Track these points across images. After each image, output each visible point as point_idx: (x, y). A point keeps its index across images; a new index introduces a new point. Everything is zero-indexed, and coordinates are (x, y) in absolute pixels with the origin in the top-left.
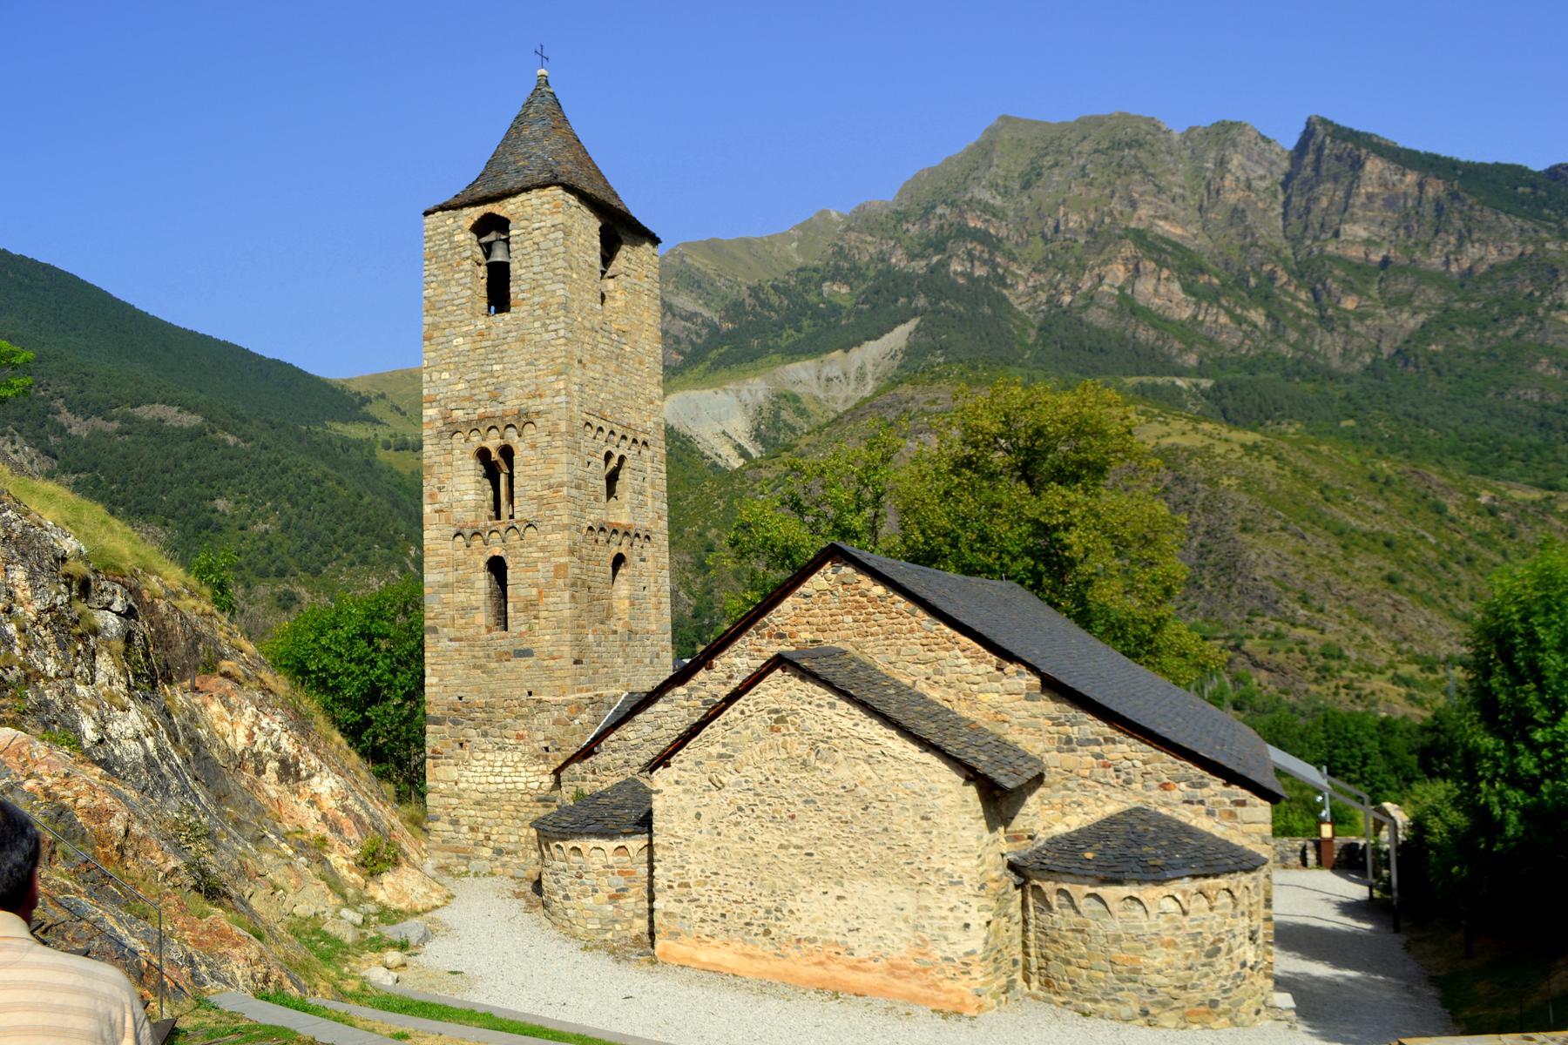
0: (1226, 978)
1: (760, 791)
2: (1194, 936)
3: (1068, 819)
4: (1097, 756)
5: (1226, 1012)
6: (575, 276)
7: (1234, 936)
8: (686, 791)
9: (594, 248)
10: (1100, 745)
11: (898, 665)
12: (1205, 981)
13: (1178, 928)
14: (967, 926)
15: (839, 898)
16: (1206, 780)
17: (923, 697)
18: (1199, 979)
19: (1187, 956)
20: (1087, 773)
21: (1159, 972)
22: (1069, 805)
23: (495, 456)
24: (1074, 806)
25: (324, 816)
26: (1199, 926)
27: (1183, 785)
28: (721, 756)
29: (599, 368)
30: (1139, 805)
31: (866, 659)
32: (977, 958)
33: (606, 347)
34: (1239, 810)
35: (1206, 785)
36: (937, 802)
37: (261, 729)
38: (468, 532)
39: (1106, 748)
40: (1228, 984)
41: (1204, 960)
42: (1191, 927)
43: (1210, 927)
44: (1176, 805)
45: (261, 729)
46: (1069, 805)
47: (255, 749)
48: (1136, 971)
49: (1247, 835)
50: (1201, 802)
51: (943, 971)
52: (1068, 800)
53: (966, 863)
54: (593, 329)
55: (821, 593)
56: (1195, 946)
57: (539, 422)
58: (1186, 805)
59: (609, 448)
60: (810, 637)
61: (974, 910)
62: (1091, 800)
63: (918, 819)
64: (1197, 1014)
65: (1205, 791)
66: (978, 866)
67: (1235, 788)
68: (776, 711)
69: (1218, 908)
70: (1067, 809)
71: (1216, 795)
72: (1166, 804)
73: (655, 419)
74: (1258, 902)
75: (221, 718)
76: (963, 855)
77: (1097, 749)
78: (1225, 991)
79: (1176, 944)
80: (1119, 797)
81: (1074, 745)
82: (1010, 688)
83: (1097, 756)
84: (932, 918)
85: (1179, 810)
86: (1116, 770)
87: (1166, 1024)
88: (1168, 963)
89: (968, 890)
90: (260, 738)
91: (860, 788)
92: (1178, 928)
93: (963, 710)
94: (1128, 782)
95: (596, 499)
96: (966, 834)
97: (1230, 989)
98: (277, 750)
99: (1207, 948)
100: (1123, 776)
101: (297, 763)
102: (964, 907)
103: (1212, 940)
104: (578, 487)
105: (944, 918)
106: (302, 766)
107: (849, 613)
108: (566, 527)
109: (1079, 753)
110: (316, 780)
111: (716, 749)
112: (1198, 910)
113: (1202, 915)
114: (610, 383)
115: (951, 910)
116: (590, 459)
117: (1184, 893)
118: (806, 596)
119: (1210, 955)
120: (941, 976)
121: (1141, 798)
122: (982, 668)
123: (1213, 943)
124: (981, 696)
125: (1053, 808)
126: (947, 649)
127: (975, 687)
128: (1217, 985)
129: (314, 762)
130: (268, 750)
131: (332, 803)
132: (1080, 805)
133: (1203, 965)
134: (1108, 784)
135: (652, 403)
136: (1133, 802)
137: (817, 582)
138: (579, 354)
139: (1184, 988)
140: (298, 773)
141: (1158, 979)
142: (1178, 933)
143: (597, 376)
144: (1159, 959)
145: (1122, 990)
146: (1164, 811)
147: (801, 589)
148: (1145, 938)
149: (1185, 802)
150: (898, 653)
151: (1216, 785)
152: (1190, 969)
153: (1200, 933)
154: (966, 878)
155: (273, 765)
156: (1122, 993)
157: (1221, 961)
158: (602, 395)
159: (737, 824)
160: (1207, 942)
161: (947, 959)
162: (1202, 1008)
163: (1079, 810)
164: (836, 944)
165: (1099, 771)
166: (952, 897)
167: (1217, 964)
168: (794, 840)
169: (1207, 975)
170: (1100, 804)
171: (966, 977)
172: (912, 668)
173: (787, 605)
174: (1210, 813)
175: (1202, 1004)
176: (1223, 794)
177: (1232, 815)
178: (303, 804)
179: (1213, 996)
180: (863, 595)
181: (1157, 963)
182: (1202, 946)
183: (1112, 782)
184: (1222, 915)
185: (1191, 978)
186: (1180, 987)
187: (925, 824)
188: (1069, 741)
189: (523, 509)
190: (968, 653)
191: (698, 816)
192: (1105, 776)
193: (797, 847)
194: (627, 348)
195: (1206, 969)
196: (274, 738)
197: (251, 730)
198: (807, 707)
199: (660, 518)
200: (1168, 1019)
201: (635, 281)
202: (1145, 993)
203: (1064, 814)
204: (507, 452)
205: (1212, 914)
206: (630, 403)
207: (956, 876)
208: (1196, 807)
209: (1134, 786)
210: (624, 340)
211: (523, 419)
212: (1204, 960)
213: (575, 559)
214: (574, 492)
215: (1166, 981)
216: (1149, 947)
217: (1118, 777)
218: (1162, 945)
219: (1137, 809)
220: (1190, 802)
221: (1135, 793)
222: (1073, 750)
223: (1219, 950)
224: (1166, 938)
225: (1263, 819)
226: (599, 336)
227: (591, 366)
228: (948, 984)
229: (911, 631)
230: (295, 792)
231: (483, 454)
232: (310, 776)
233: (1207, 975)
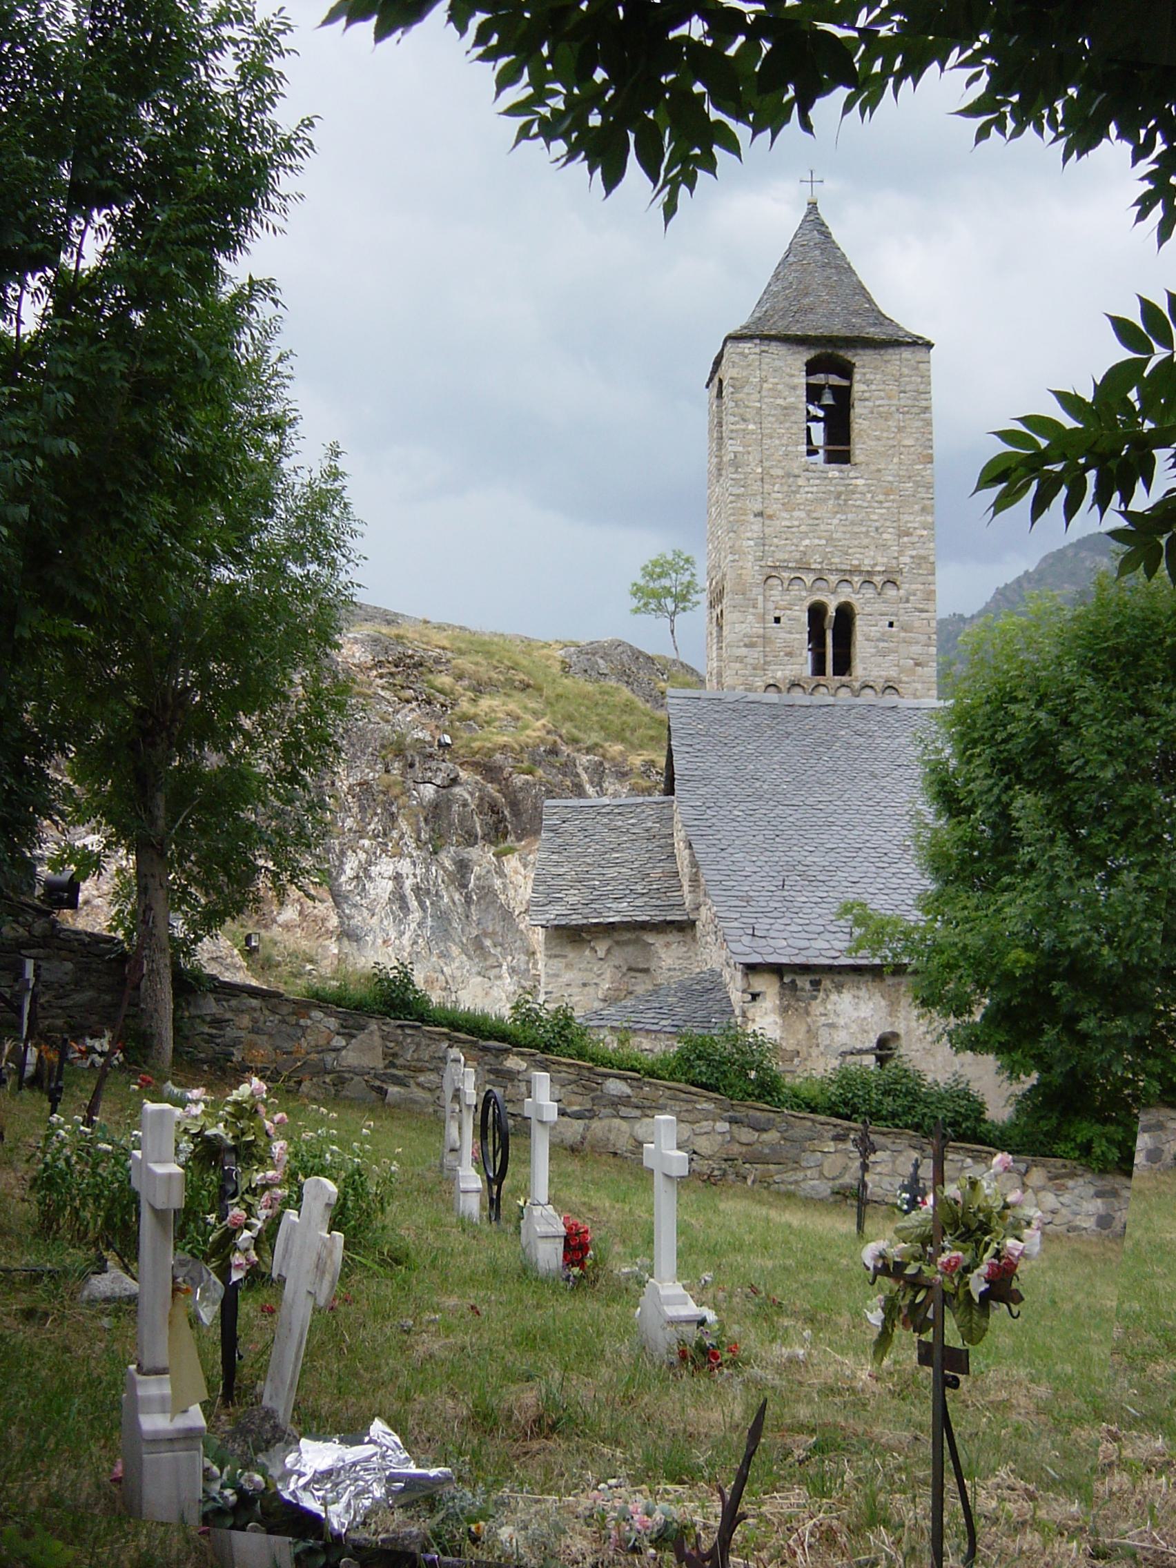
6: (751, 427)
9: (794, 388)
29: (803, 515)
33: (815, 489)
54: (788, 475)
73: (914, 553)
95: (789, 654)
114: (822, 527)
135: (908, 534)
138: (757, 507)
143: (796, 523)
158: (807, 542)
199: (917, 664)
201: (878, 403)
206: (866, 541)
210: (852, 474)
226: (801, 482)
227: (785, 515)
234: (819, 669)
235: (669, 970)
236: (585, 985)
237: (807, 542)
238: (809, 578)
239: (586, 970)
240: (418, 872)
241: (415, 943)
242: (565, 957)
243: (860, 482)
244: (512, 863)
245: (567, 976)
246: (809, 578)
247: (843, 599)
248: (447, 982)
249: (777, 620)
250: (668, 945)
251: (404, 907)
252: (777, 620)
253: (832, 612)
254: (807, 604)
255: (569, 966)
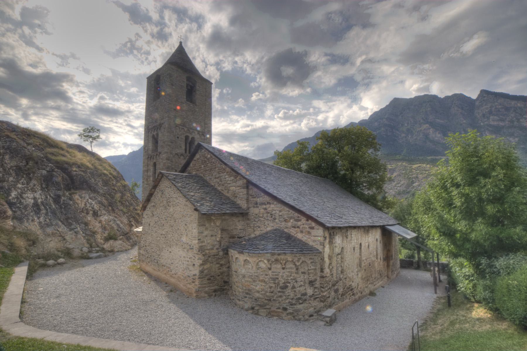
0: (292, 299)
1: (159, 217)
2: (274, 279)
3: (255, 233)
4: (265, 209)
5: (291, 314)
7: (296, 282)
8: (148, 217)
10: (266, 205)
11: (212, 179)
12: (280, 299)
13: (267, 275)
14: (194, 265)
15: (170, 252)
16: (300, 219)
17: (216, 189)
18: (277, 298)
19: (271, 287)
20: (261, 215)
21: (258, 292)
22: (256, 227)
23: (155, 136)
24: (257, 227)
25: (102, 226)
26: (276, 275)
27: (291, 221)
28: (153, 206)
30: (277, 228)
31: (205, 178)
32: (197, 277)
34: (311, 231)
35: (300, 220)
36: (188, 219)
37: (89, 203)
38: (150, 156)
39: (268, 206)
40: (294, 302)
41: (279, 290)
42: (272, 275)
43: (282, 276)
44: (290, 228)
45: (89, 203)
46: (256, 227)
47: (87, 208)
48: (249, 290)
49: (314, 241)
50: (298, 227)
51: (187, 281)
52: (255, 225)
53: (194, 242)
55: (198, 159)
56: (275, 283)
57: (163, 126)
58: (293, 228)
59: (187, 134)
60: (194, 173)
61: (196, 259)
62: (263, 226)
63: (184, 225)
64: (276, 312)
65: (299, 223)
66: (198, 243)
67: (310, 221)
68: (162, 191)
69: (287, 269)
70: (255, 229)
71: (303, 224)
72: (287, 228)
74: (315, 269)
75: (78, 199)
76: (194, 239)
77: (265, 206)
78: (292, 305)
79: (265, 281)
80: (272, 225)
81: (258, 205)
82: (238, 184)
83: (265, 209)
84: (186, 261)
85: (291, 230)
86: (271, 215)
87: (262, 314)
88: (262, 289)
89: (195, 251)
90: (88, 205)
91: (175, 215)
92: (267, 275)
93: (225, 193)
94: (275, 219)
96: (195, 231)
97: (295, 304)
98: (93, 208)
99: (281, 285)
100: (273, 217)
101: (98, 211)
102: (193, 258)
103: (283, 282)
104: (172, 142)
105: (188, 261)
106: (99, 213)
107: (203, 164)
108: (167, 153)
109: (260, 208)
110: (102, 217)
111: (153, 204)
112: (276, 268)
113: (278, 271)
115: (190, 258)
116: (178, 136)
117: (268, 260)
118: (195, 161)
119: (282, 288)
120: (187, 282)
121: (278, 225)
122: (232, 178)
123: (284, 283)
124: (231, 188)
125: (251, 228)
126: (223, 173)
127: (229, 185)
128: (287, 301)
129: (104, 212)
130: (91, 208)
131: (104, 223)
132: (259, 227)
133: (279, 292)
134: (268, 220)
136: (276, 226)
137: (197, 156)
139: (270, 300)
140: (98, 214)
141: (257, 295)
142: (266, 277)
144: (258, 287)
145: (246, 297)
146: (286, 230)
147: (195, 159)
148: (253, 277)
149: (293, 227)
150: (212, 176)
151: (304, 220)
152: (272, 292)
153: (278, 278)
154: (194, 247)
155: (91, 212)
156: (246, 299)
157: (288, 291)
159: (155, 227)
160: (281, 283)
161: (189, 276)
162: (279, 310)
163: (259, 229)
164: (169, 268)
165: (265, 215)
166: (190, 254)
167: (286, 293)
168: (164, 233)
169: (281, 296)
170: (265, 227)
171: (193, 284)
172: (215, 181)
173: (191, 165)
174: (302, 232)
175: (279, 308)
176: (306, 224)
177: (309, 233)
178: (97, 222)
179: (285, 306)
180: (206, 158)
181: (257, 288)
182: (278, 284)
183: (269, 219)
184: (289, 272)
185: (273, 297)
186: (267, 300)
187: (186, 227)
188: (256, 204)
189: (160, 150)
190: (228, 174)
191: (149, 225)
192: (267, 217)
193: (164, 235)
194: (197, 109)
195: (280, 294)
196: (92, 205)
197: (86, 202)
198: (167, 188)
200: (263, 312)
202: (253, 300)
203: (254, 231)
204: (157, 135)
205: (284, 271)
207: (192, 246)
208: (297, 229)
209: (276, 221)
211: (161, 125)
212: (279, 290)
213: (169, 161)
214: (170, 144)
215: (261, 296)
216: (254, 281)
217: (272, 217)
218: (259, 281)
219: (276, 230)
220: (294, 227)
221: (277, 224)
222: (257, 207)
223: (287, 287)
224: (261, 278)
225: (320, 235)
228: (189, 286)
229: (215, 168)
230: (95, 219)
231: (153, 136)
232: (100, 216)
233: (281, 296)
234: (186, 152)
235: (240, 230)
236: (212, 236)
237: (185, 120)
238: (186, 129)
239: (212, 230)
240: (43, 197)
241: (45, 221)
242: (205, 225)
243: (197, 109)
244: (76, 197)
245: (206, 233)
246: (186, 129)
247: (193, 136)
248: (60, 234)
249: (178, 138)
250: (239, 221)
251: (39, 209)
252: (178, 138)
253: (190, 139)
254: (185, 135)
255: (207, 229)
